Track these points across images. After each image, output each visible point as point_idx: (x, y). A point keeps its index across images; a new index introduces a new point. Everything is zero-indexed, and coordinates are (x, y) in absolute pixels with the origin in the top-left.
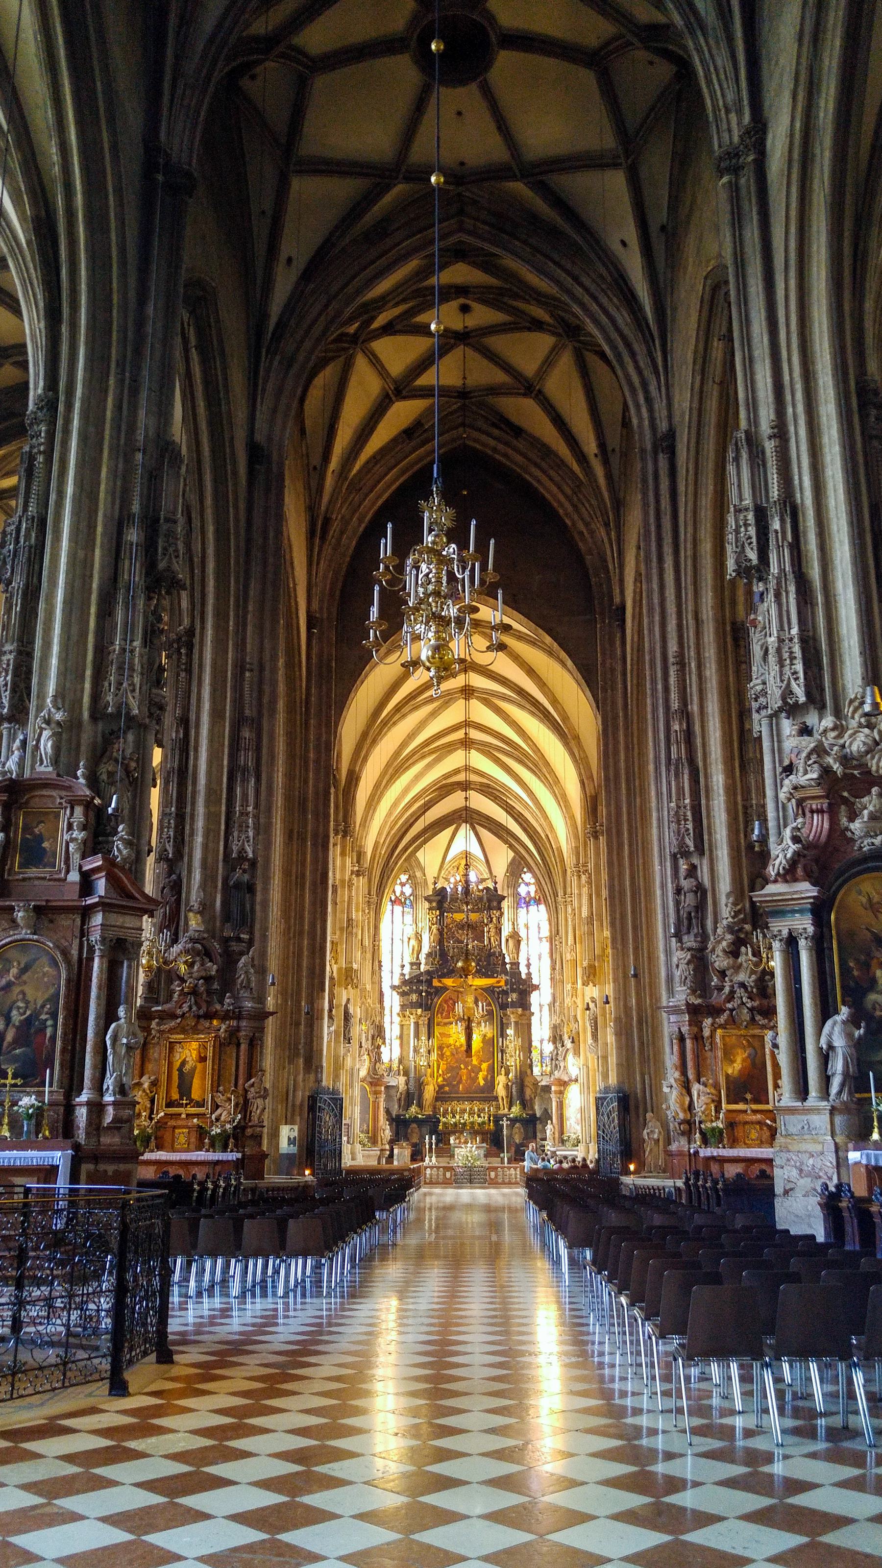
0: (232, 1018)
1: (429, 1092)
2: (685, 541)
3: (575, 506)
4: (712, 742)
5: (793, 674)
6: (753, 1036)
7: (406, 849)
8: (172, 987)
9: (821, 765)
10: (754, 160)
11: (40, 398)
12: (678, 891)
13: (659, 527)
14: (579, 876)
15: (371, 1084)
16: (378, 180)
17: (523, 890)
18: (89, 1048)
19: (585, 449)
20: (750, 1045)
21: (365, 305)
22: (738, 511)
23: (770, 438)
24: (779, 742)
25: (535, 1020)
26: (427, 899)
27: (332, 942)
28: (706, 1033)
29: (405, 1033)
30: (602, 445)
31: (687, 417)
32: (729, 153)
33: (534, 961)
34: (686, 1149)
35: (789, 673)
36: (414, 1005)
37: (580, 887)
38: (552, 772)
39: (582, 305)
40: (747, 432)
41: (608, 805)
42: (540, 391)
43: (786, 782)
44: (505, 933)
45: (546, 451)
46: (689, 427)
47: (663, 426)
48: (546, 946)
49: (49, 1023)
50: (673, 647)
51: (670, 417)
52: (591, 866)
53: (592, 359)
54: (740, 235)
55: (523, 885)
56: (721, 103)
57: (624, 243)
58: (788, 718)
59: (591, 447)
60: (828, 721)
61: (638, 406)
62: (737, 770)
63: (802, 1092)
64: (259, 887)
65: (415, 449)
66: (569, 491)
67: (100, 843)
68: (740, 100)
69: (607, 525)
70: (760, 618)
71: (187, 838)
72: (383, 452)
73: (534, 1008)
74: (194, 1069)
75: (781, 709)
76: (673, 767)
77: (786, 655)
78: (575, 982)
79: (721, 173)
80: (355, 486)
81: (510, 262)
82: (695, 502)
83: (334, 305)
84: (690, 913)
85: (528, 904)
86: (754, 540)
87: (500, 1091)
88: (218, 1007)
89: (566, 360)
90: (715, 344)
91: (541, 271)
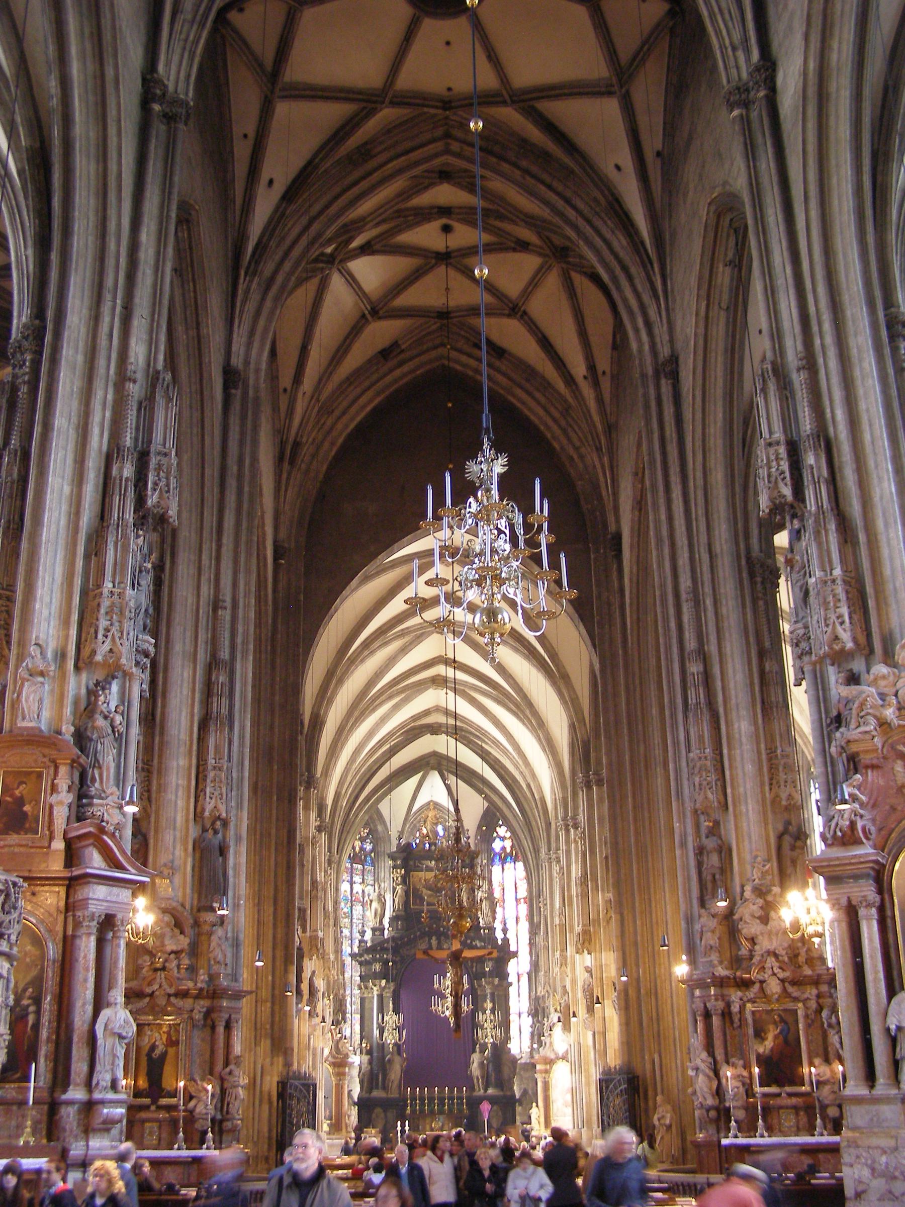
0: (203, 998)
1: (396, 1072)
2: (694, 469)
3: (564, 431)
4: (732, 685)
5: (838, 618)
6: (785, 1010)
7: (368, 799)
8: (140, 961)
9: (875, 717)
10: (766, 96)
11: (25, 326)
12: (700, 851)
13: (664, 454)
14: (567, 831)
15: (334, 1065)
16: (365, 104)
17: (497, 845)
18: (75, 1039)
19: (573, 372)
20: (783, 1020)
21: (345, 225)
22: (770, 445)
23: (798, 370)
24: (824, 690)
25: (513, 991)
26: (392, 857)
27: (299, 909)
28: (735, 1008)
29: (367, 1005)
30: (592, 367)
31: (692, 343)
32: (738, 89)
33: (511, 924)
34: (715, 1139)
35: (833, 617)
36: (376, 976)
37: (568, 842)
38: (535, 713)
39: (575, 227)
40: (773, 363)
41: (608, 754)
42: (525, 313)
43: (838, 735)
44: (480, 895)
45: (530, 372)
46: (695, 353)
47: (664, 351)
48: (523, 909)
49: (32, 1009)
50: (685, 582)
51: (672, 341)
52: (582, 818)
53: (581, 282)
54: (755, 167)
55: (497, 840)
56: (727, 42)
57: (618, 168)
58: (833, 665)
59: (579, 369)
60: (881, 669)
61: (637, 330)
62: (760, 716)
63: (870, 1077)
64: (232, 851)
65: (391, 371)
66: (557, 415)
67: (83, 806)
68: (746, 40)
69: (599, 449)
70: (798, 558)
71: (154, 795)
72: (358, 373)
73: (512, 978)
74: (164, 1056)
75: (826, 656)
76: (691, 715)
77: (830, 598)
78: (564, 949)
79: (731, 107)
80: (326, 409)
81: (497, 185)
82: (704, 428)
83: (316, 227)
84: (714, 876)
85: (503, 862)
86: (787, 474)
87: (475, 1069)
88: (190, 984)
89: (553, 281)
90: (721, 269)
91: (532, 193)
